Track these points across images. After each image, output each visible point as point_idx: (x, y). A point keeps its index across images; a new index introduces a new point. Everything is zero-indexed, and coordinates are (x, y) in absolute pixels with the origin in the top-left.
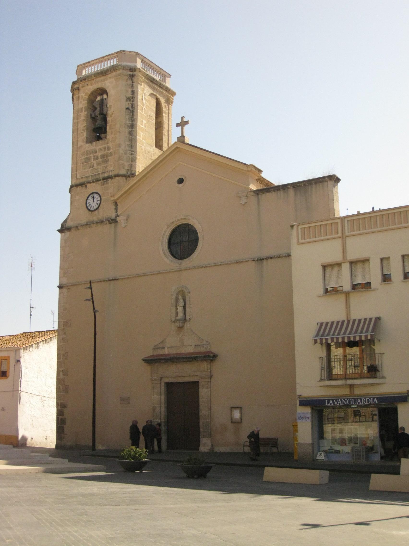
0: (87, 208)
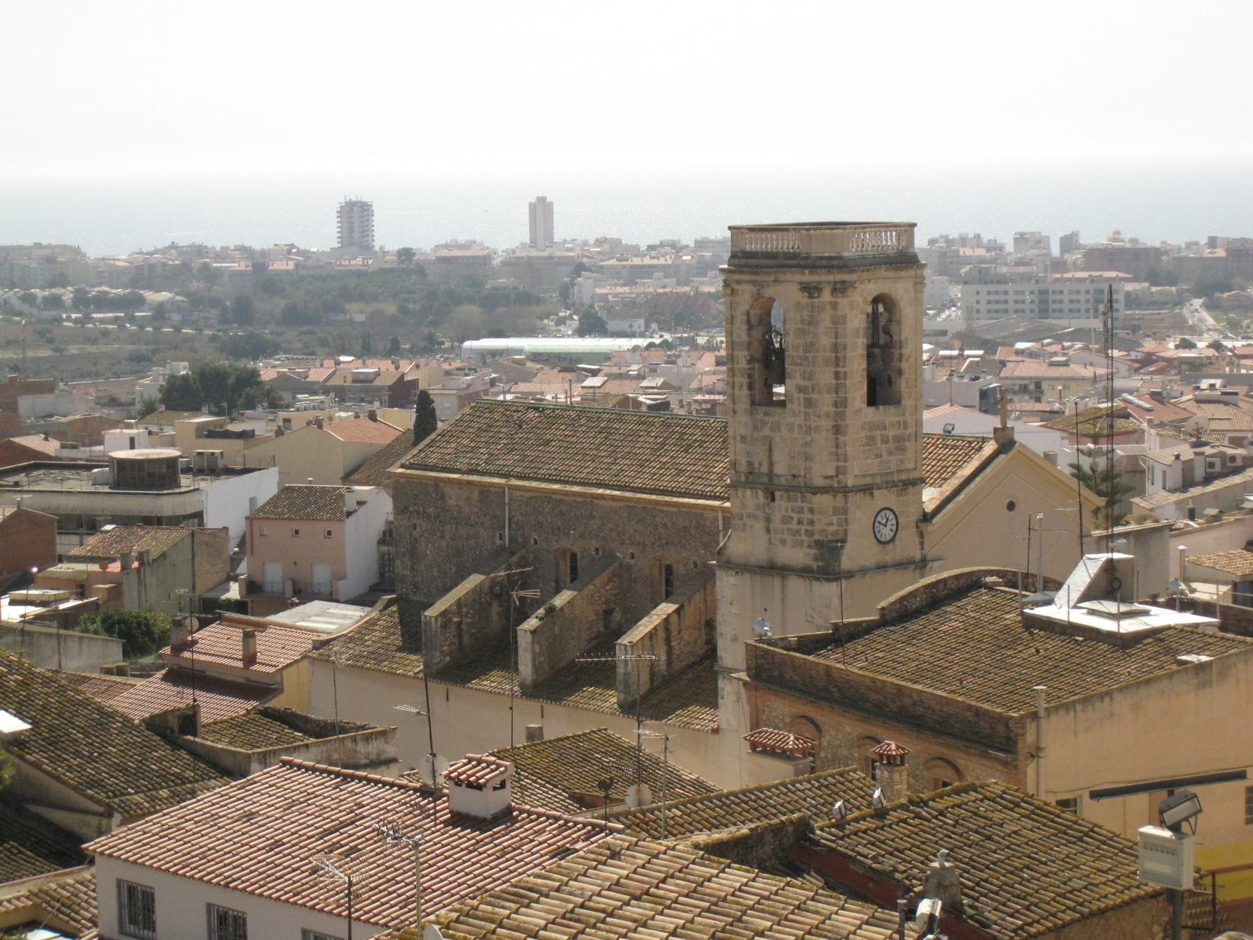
0: (878, 540)
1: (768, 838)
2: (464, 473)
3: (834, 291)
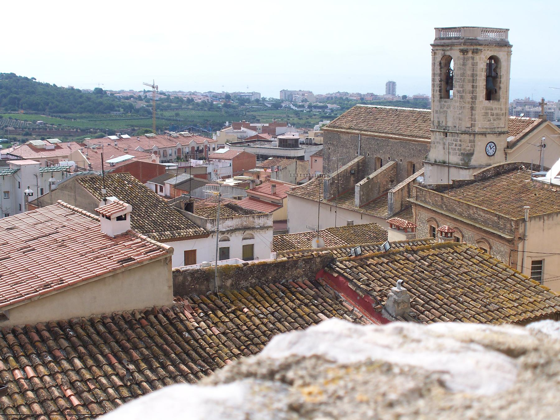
1: (300, 263)
2: (347, 129)
3: (473, 53)
